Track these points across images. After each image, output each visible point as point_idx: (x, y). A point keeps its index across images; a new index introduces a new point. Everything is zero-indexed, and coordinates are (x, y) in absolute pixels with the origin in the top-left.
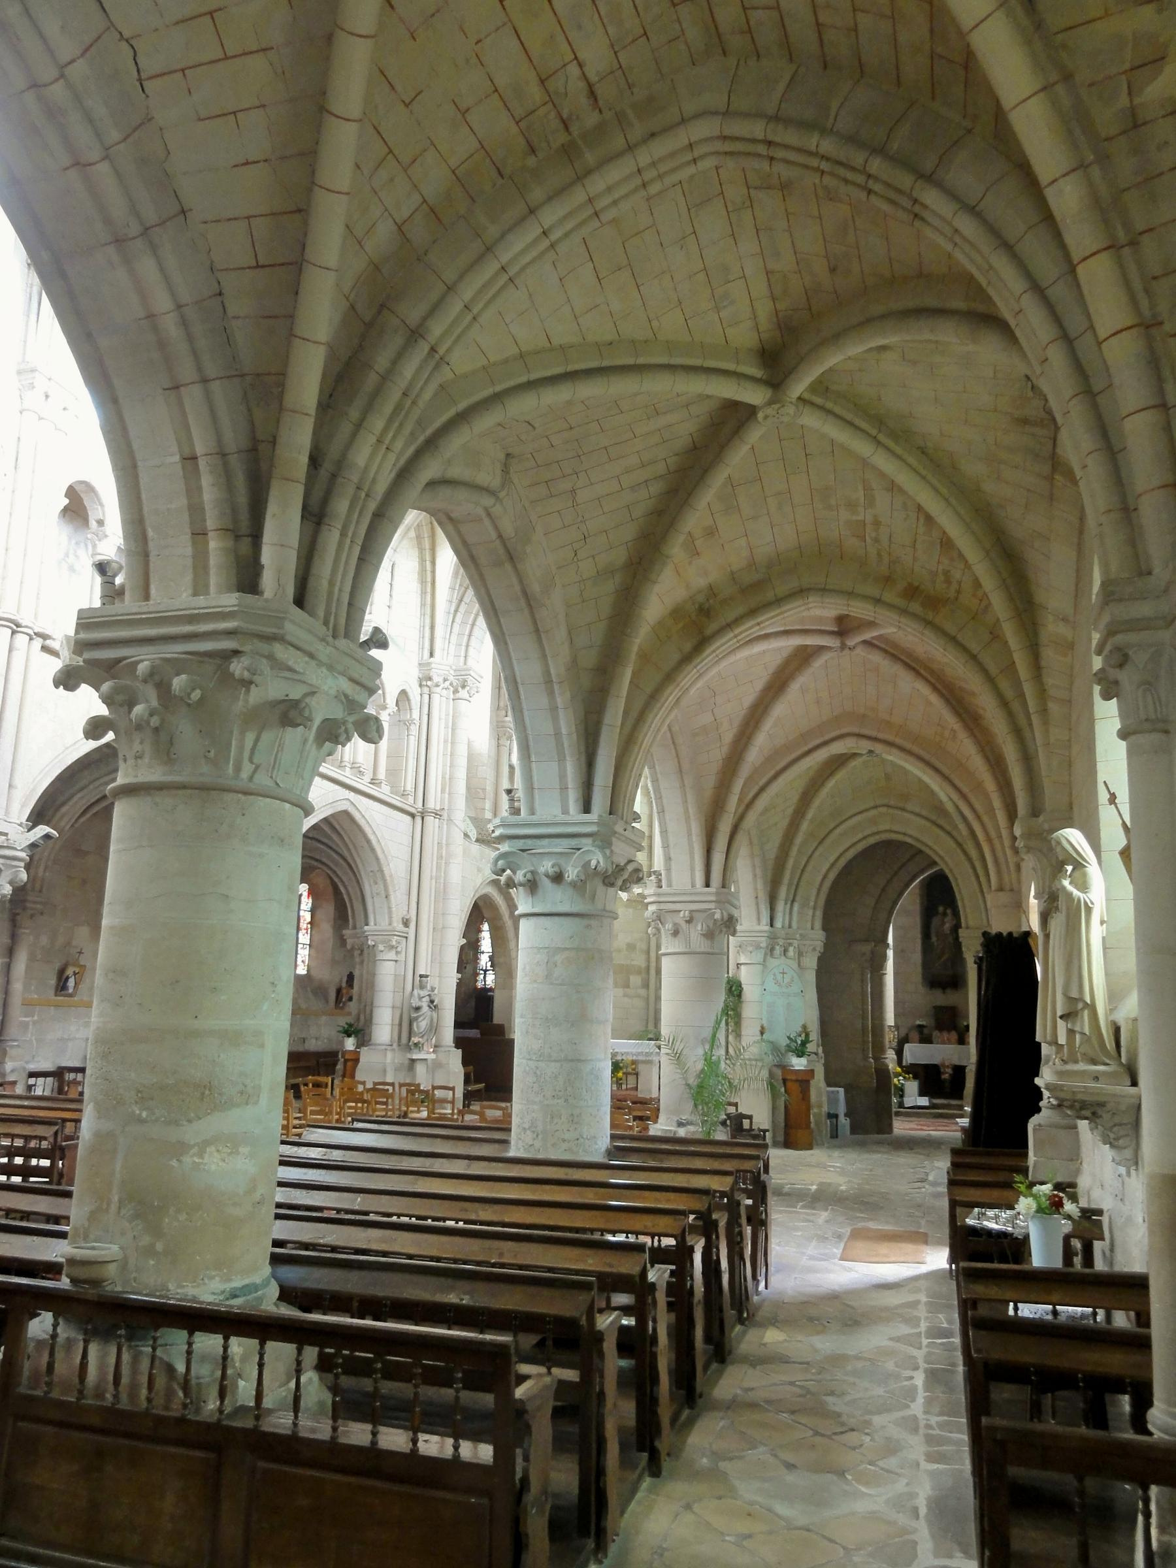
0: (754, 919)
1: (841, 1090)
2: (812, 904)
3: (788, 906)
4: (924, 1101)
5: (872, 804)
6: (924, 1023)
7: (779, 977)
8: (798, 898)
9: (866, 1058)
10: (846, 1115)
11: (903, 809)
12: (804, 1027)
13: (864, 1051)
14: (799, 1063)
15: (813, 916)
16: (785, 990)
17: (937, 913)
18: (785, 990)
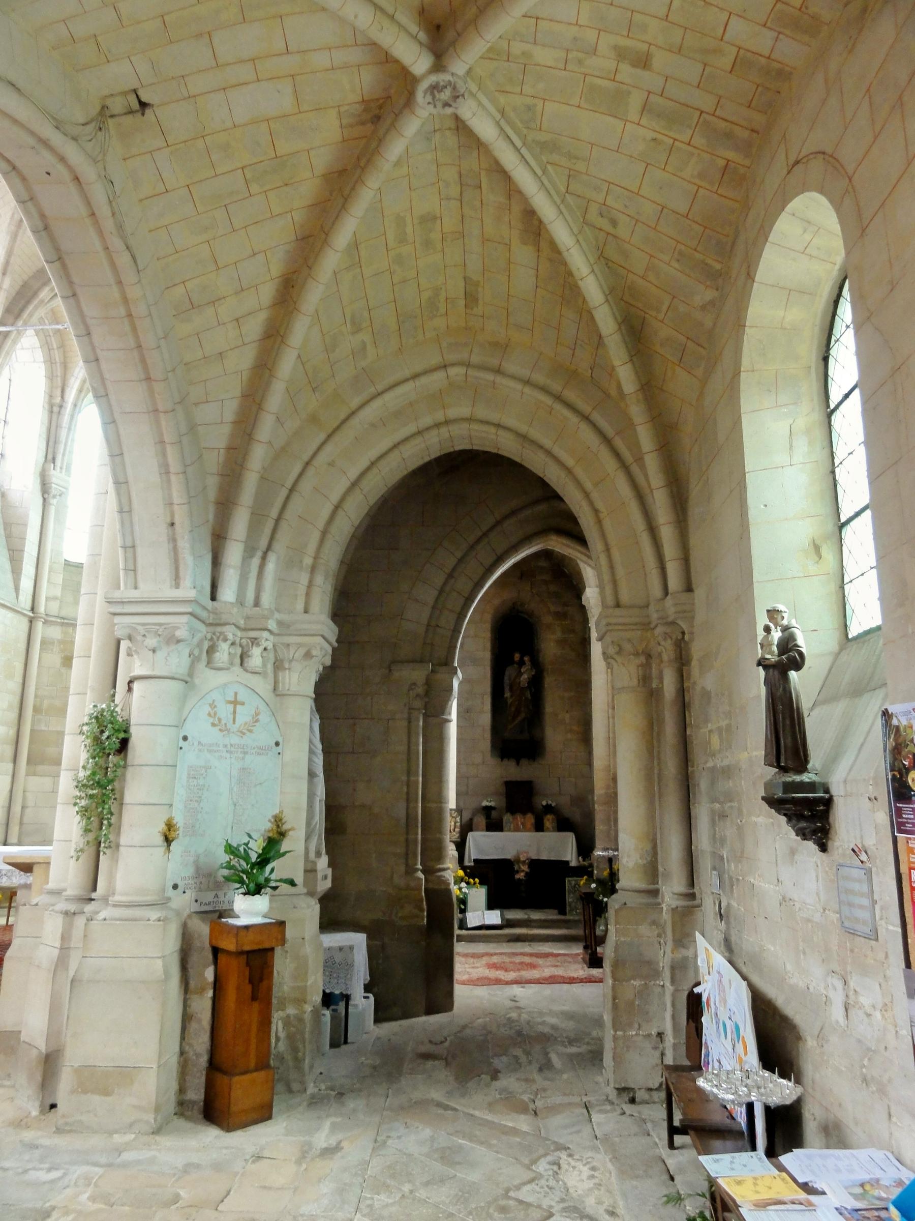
0: (166, 574)
1: (358, 940)
2: (308, 561)
3: (256, 562)
4: (494, 917)
5: (436, 360)
6: (492, 804)
7: (225, 711)
8: (276, 546)
9: (410, 871)
10: (368, 988)
11: (498, 371)
12: (278, 820)
13: (408, 855)
14: (249, 910)
15: (310, 585)
16: (235, 740)
17: (512, 662)
18: (235, 740)
